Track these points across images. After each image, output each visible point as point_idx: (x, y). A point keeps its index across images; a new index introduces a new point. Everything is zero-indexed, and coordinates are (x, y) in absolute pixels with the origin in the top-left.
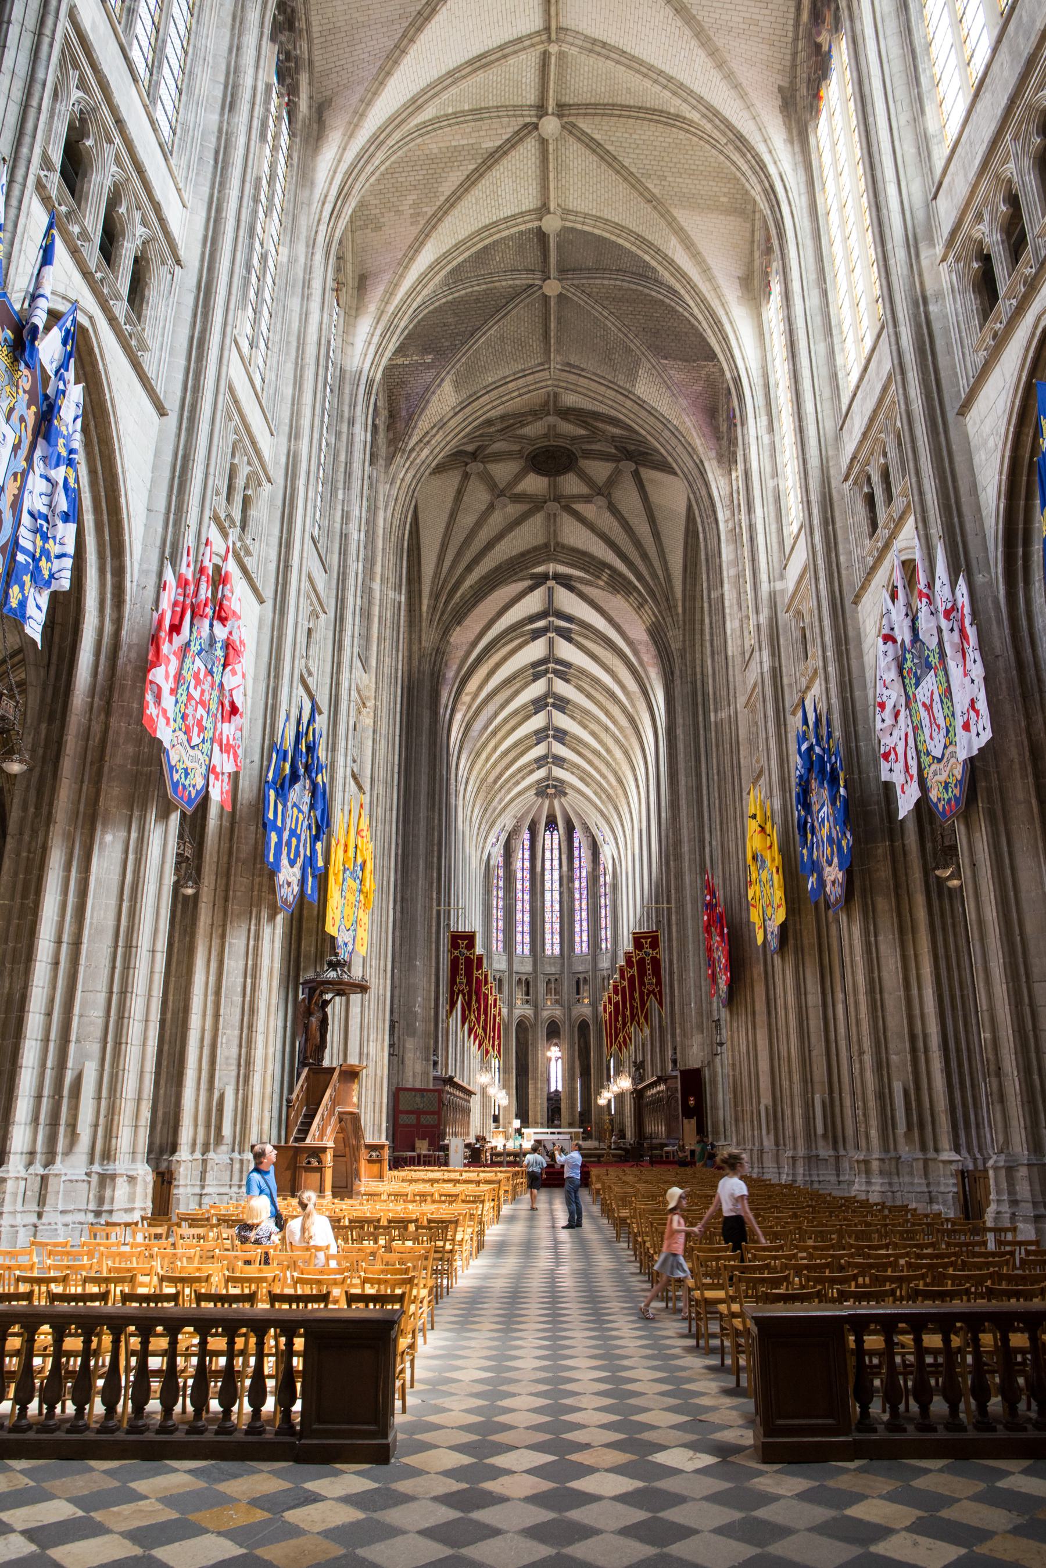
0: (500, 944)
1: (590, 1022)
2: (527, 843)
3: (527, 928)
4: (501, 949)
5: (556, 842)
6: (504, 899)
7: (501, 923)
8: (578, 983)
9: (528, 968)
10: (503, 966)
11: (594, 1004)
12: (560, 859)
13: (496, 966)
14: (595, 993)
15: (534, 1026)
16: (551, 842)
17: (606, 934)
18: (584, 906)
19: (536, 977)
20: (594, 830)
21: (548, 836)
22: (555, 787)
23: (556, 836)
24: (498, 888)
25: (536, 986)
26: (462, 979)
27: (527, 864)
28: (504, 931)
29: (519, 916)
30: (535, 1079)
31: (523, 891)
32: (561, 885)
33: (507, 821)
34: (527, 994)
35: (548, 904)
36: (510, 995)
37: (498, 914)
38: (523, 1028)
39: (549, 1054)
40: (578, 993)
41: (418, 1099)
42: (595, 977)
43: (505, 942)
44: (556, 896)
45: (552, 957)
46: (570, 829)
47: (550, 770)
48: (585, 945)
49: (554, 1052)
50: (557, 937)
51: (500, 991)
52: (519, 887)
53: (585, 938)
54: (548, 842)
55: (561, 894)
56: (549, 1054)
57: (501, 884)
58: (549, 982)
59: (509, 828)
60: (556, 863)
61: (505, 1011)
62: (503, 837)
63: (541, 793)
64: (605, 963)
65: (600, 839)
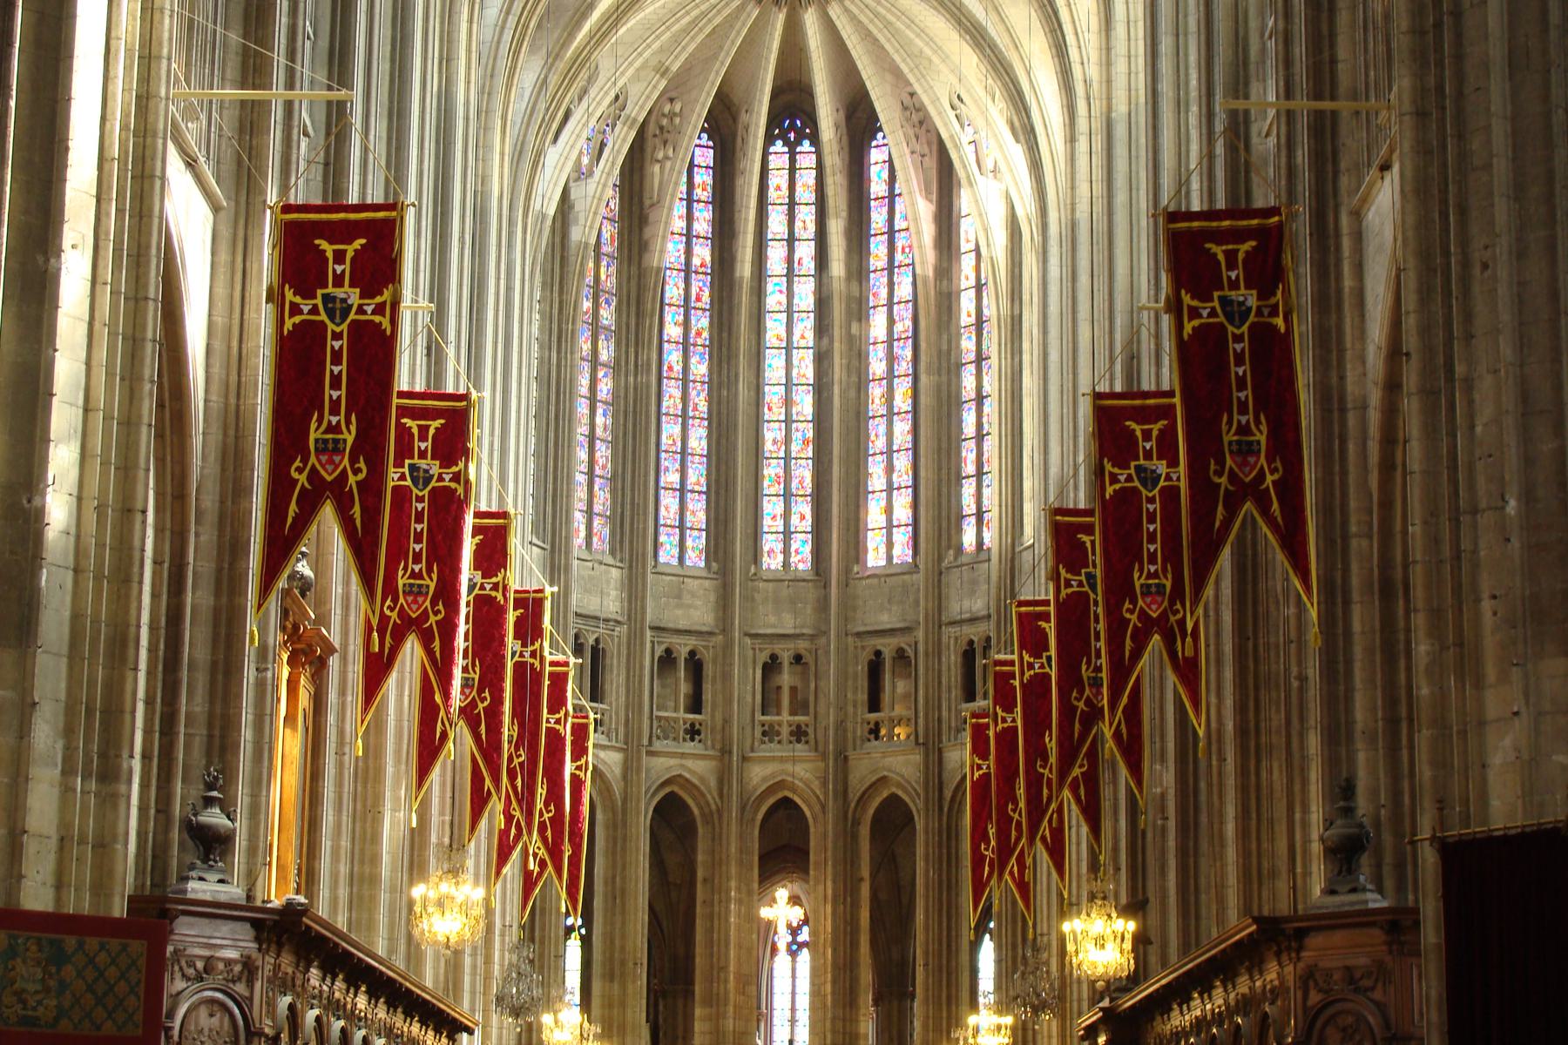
1: (916, 806)
2: (703, 178)
3: (697, 475)
4: (601, 543)
5: (807, 179)
6: (617, 368)
7: (603, 452)
9: (698, 612)
10: (610, 603)
11: (931, 746)
14: (934, 704)
15: (714, 818)
18: (902, 402)
19: (728, 646)
20: (947, 127)
23: (807, 160)
24: (596, 329)
25: (726, 677)
26: (333, 424)
27: (703, 253)
28: (617, 482)
29: (671, 430)
30: (715, 1001)
31: (686, 346)
32: (822, 329)
33: (627, 72)
34: (695, 705)
35: (773, 395)
36: (633, 705)
37: (593, 419)
38: (673, 817)
39: (765, 913)
40: (874, 704)
41: (27, 974)
42: (937, 649)
44: (805, 367)
45: (786, 577)
46: (861, 124)
48: (902, 537)
49: (781, 910)
50: (803, 509)
51: (596, 695)
52: (673, 331)
53: (903, 512)
54: (778, 180)
55: (822, 359)
56: (765, 913)
57: (607, 316)
58: (771, 667)
59: (637, 111)
60: (806, 252)
61: (612, 760)
64: (971, 601)
65: (963, 158)
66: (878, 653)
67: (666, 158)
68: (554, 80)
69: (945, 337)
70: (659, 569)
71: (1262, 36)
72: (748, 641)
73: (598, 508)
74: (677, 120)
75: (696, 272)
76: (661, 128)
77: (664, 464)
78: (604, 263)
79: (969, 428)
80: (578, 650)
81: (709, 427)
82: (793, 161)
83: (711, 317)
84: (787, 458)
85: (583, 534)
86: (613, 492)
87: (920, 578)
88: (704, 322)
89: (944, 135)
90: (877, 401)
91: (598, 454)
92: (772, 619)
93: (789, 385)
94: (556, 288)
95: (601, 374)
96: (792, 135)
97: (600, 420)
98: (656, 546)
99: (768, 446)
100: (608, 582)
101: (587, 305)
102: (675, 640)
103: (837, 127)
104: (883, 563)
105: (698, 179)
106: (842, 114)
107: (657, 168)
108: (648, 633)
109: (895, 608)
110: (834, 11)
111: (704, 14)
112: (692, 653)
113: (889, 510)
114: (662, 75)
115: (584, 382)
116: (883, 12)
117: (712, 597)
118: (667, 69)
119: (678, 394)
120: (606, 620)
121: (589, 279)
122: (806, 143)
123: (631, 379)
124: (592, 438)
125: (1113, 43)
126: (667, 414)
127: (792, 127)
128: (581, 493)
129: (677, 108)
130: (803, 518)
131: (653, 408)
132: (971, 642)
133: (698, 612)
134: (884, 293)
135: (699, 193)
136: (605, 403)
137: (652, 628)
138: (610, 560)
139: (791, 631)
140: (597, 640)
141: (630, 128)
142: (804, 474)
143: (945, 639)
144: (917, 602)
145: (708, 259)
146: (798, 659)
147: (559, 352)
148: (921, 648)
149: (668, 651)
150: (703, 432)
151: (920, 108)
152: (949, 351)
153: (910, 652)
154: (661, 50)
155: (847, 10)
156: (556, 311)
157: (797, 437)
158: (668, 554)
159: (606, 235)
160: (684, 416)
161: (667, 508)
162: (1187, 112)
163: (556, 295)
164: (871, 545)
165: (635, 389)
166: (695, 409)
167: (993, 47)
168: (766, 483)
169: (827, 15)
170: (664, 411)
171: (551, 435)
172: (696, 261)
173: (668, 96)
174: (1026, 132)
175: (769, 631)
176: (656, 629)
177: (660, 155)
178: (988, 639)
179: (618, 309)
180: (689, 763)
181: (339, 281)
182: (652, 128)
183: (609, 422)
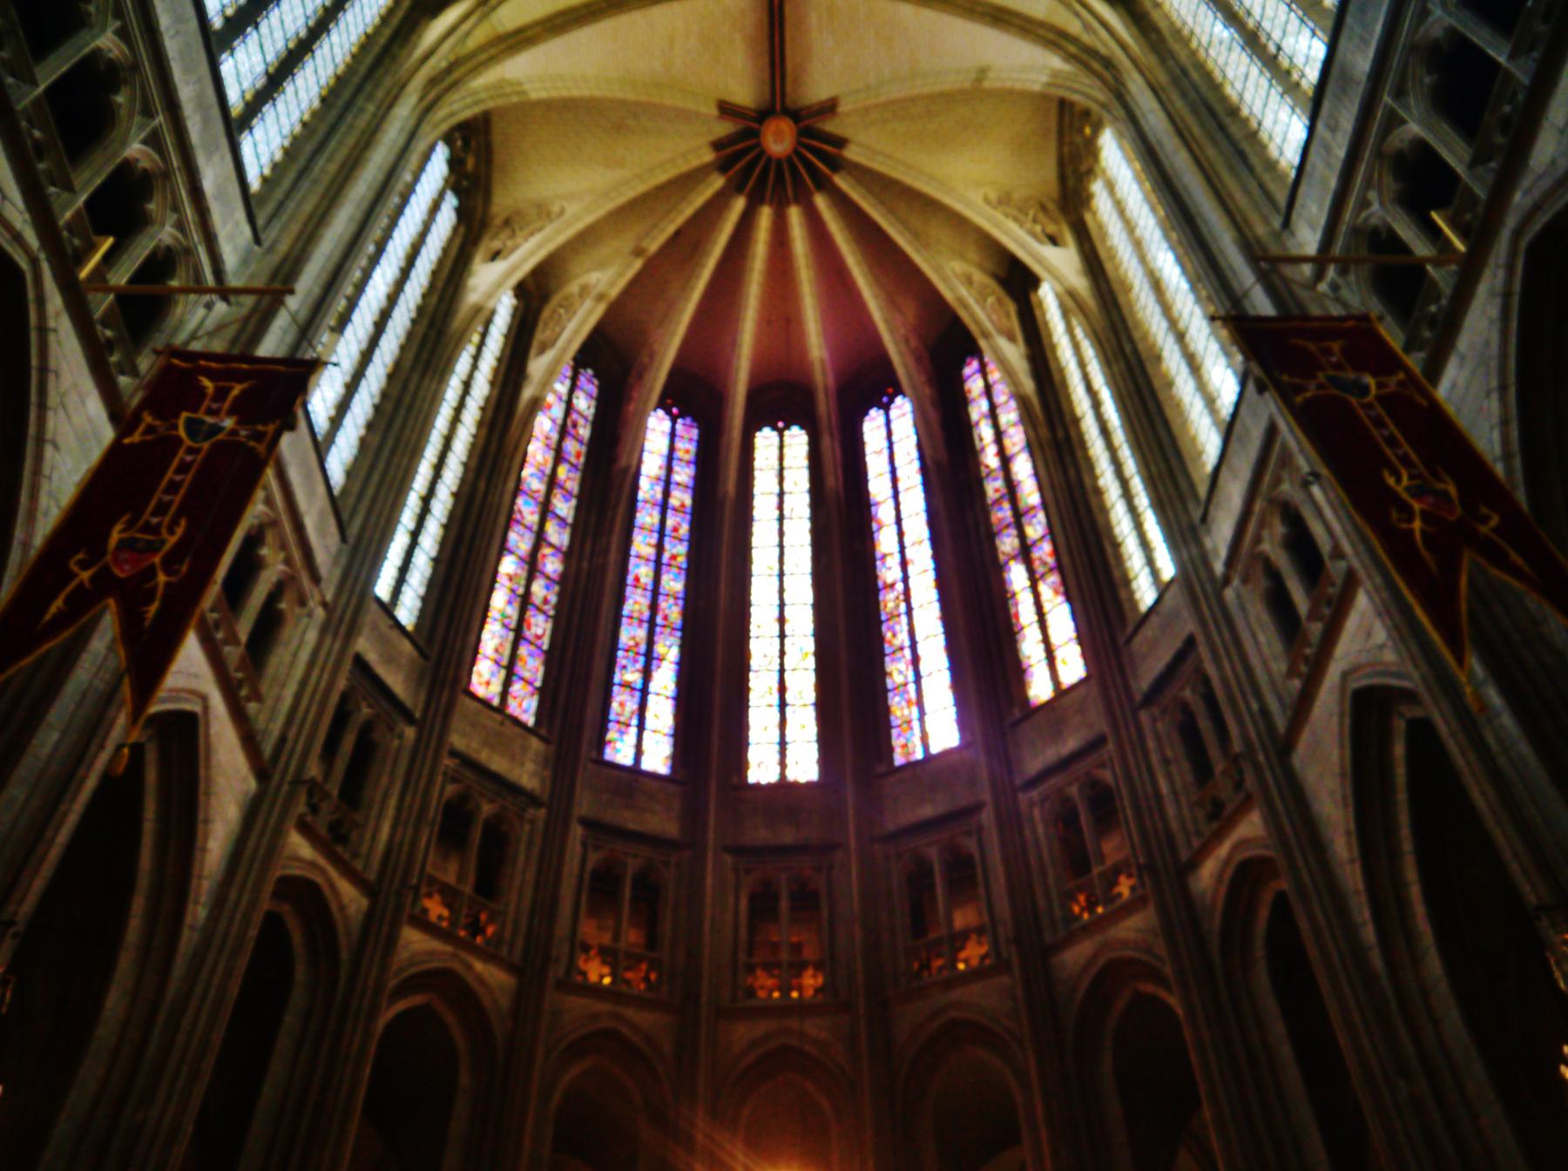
6: (568, 556)
8: (919, 878)
16: (781, 463)
21: (765, 440)
31: (658, 567)
42: (1010, 821)
58: (763, 905)
72: (728, 859)
88: (681, 549)
108: (577, 831)
123: (585, 564)
132: (1066, 801)
137: (586, 823)
143: (1023, 807)
153: (971, 845)
158: (621, 751)
161: (622, 704)
176: (586, 823)
180: (630, 1013)
183: (553, 599)
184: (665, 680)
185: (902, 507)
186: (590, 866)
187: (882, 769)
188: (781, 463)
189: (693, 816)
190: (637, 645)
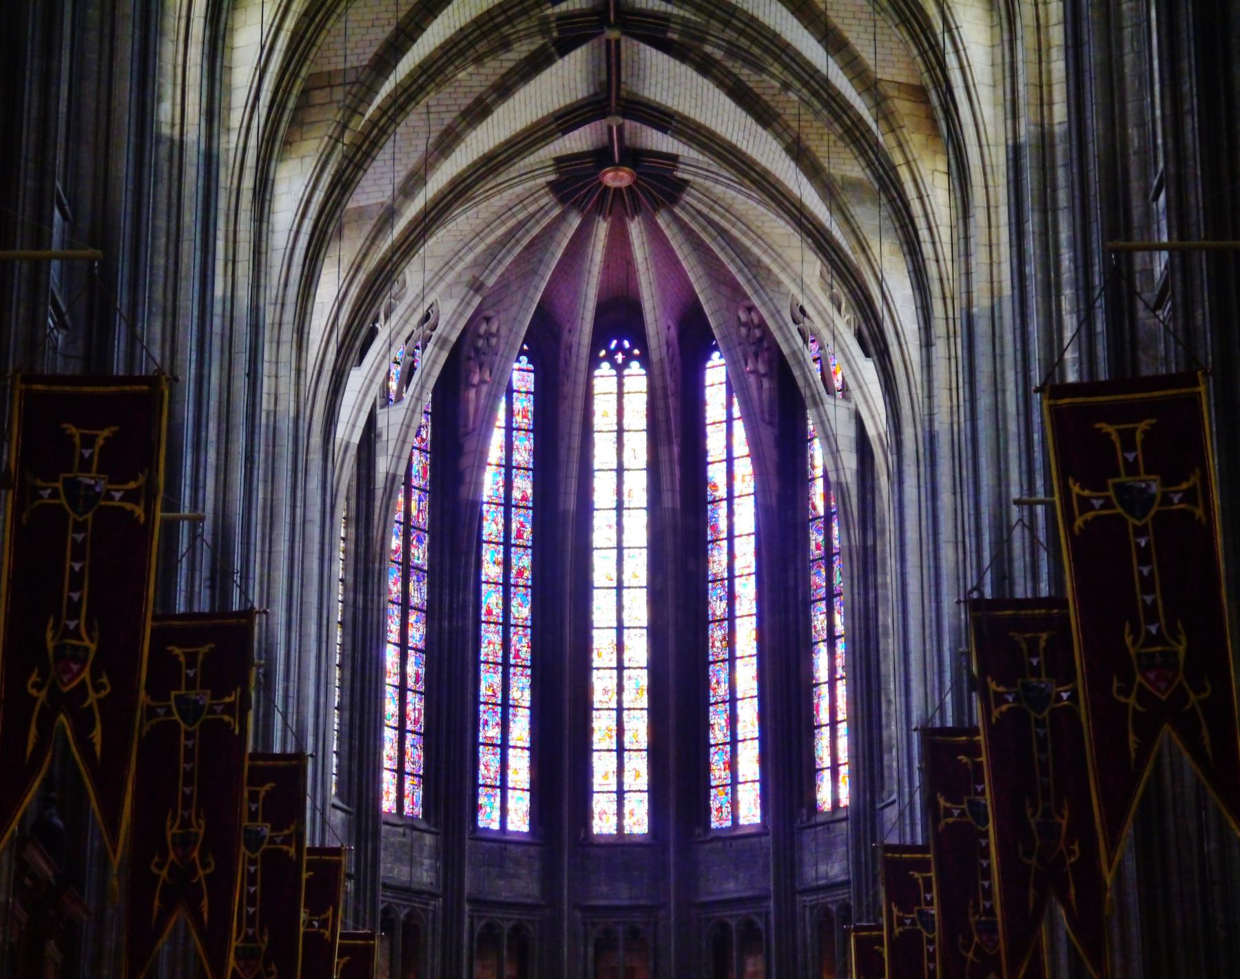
0: (414, 791)
4: (414, 805)
6: (431, 613)
7: (415, 704)
9: (524, 885)
10: (425, 875)
12: (653, 468)
13: (392, 870)
17: (832, 746)
20: (789, 341)
21: (604, 380)
22: (635, 157)
27: (523, 486)
28: (430, 739)
29: (489, 681)
31: (506, 587)
35: (603, 641)
43: (429, 780)
44: (638, 609)
45: (621, 844)
46: (693, 342)
47: (612, 62)
52: (491, 570)
57: (420, 555)
58: (605, 943)
60: (637, 486)
62: (431, 362)
63: (575, 184)
66: (724, 927)
67: (482, 382)
68: (354, 291)
69: (791, 573)
70: (479, 834)
71: (1146, 196)
73: (408, 767)
74: (494, 341)
75: (517, 507)
76: (477, 350)
77: (483, 717)
78: (415, 497)
79: (822, 673)
80: (388, 923)
81: (532, 676)
82: (620, 385)
83: (533, 554)
84: (620, 710)
85: (393, 795)
86: (426, 749)
87: (768, 841)
88: (526, 561)
89: (785, 350)
90: (718, 644)
91: (410, 708)
92: (604, 889)
93: (620, 628)
94: (362, 525)
95: (412, 618)
96: (619, 357)
97: (411, 669)
98: (476, 808)
99: (598, 698)
100: (421, 850)
101: (396, 542)
102: (497, 915)
103: (668, 344)
104: (729, 824)
105: (517, 406)
106: (673, 331)
107: (472, 394)
108: (467, 907)
109: (741, 875)
110: (662, 220)
111: (521, 224)
112: (517, 929)
113: (732, 765)
114: (477, 291)
115: (394, 626)
116: (716, 218)
117: (537, 865)
118: (482, 285)
119: (497, 639)
120: (419, 893)
121: (399, 516)
122: (635, 366)
123: (446, 624)
124: (402, 689)
125: (972, 231)
126: (486, 662)
127: (620, 347)
128: (389, 750)
129: (494, 329)
130: (638, 775)
131: (470, 655)
133: (524, 885)
134: (723, 525)
135: (519, 420)
136: (416, 649)
137: (470, 901)
138: (423, 826)
139: (626, 903)
140: (409, 916)
141: (441, 348)
142: (638, 729)
144: (766, 866)
145: (529, 492)
146: (634, 933)
147: (365, 595)
148: (772, 918)
149: (490, 927)
150: (526, 682)
151: (762, 324)
152: (796, 587)
153: (761, 924)
154: (475, 263)
155: (676, 219)
156: (362, 550)
157: (626, 683)
158: (489, 818)
159: (416, 468)
160: (506, 665)
161: (486, 766)
162: (1058, 296)
163: (362, 531)
164: (714, 805)
165: (450, 633)
166: (517, 656)
167: (837, 248)
168: (596, 737)
169: (656, 224)
170: (482, 658)
171: (358, 685)
172: (516, 494)
173: (480, 316)
174: (874, 342)
175: (602, 902)
176: (473, 901)
177: (476, 379)
178: (847, 908)
179: (431, 548)
181: (85, 466)
182: (467, 350)
183: (422, 671)
184: (520, 729)
185: (736, 519)
186: (477, 931)
187: (699, 831)
188: (619, 401)
189: (550, 876)
190: (494, 695)
